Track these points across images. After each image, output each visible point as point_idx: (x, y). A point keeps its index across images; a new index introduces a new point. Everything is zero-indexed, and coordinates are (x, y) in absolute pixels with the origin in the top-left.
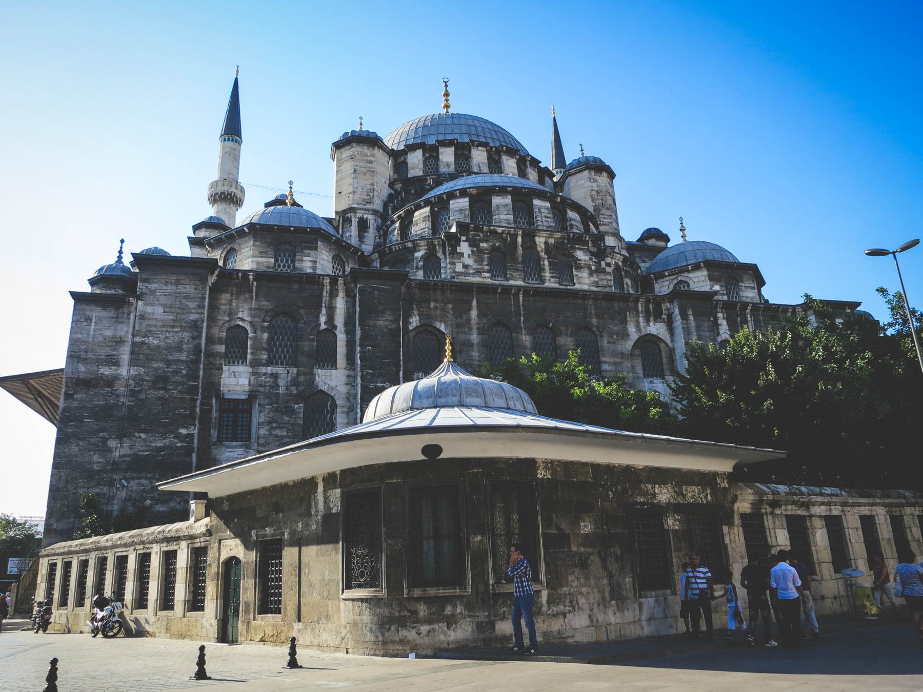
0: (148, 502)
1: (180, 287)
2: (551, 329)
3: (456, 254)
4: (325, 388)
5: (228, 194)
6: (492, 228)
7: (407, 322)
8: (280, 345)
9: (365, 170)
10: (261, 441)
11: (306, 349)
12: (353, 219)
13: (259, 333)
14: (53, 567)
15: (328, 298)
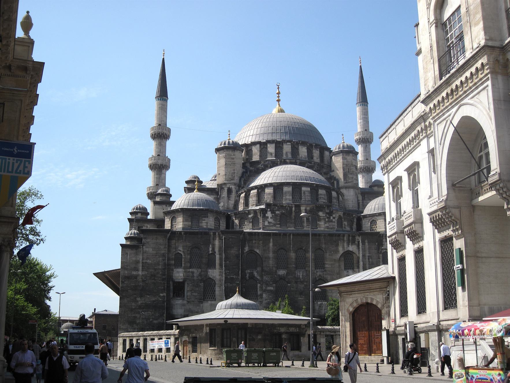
0: (151, 320)
1: (157, 240)
2: (304, 250)
3: (265, 217)
4: (212, 277)
5: (162, 134)
6: (281, 205)
7: (243, 249)
8: (194, 260)
9: (230, 163)
10: (188, 297)
11: (204, 261)
12: (225, 189)
14: (125, 341)
15: (212, 240)
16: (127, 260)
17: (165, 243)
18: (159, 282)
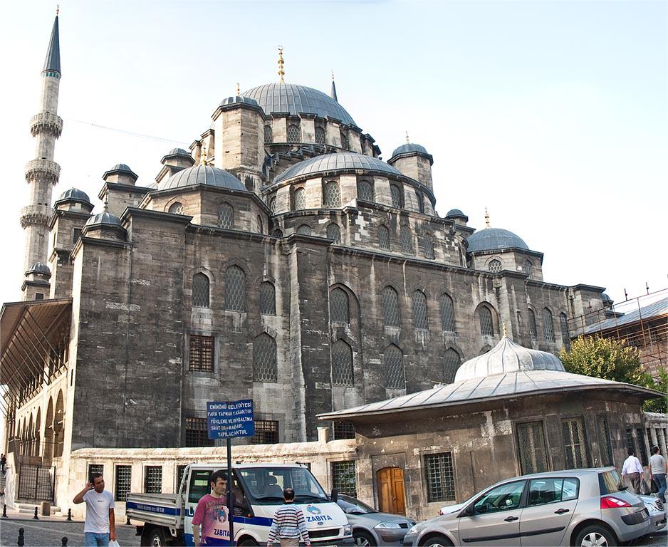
10: (223, 373)
11: (253, 297)
12: (241, 178)
13: (217, 281)
16: (96, 274)
17: (179, 247)
18: (167, 331)
